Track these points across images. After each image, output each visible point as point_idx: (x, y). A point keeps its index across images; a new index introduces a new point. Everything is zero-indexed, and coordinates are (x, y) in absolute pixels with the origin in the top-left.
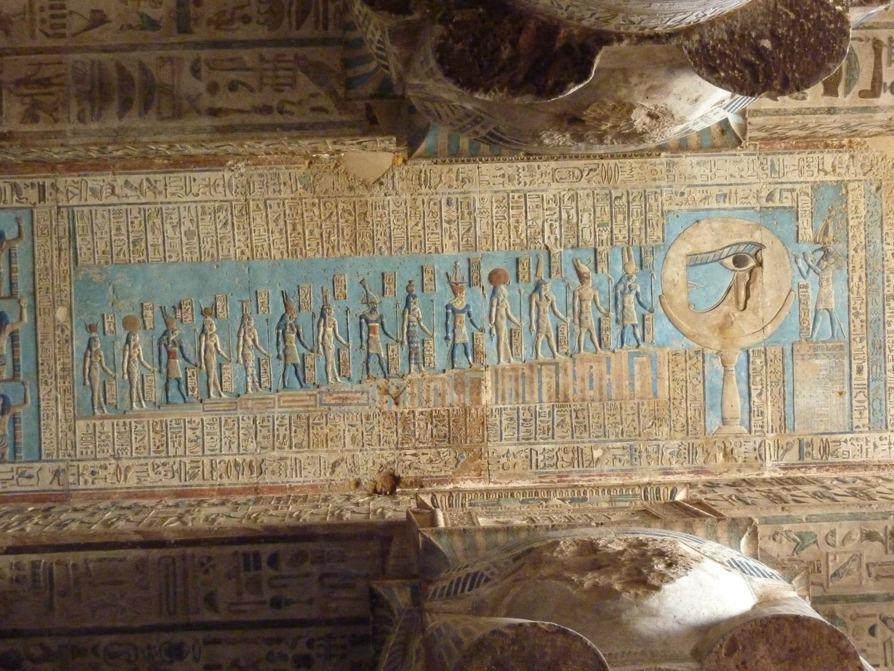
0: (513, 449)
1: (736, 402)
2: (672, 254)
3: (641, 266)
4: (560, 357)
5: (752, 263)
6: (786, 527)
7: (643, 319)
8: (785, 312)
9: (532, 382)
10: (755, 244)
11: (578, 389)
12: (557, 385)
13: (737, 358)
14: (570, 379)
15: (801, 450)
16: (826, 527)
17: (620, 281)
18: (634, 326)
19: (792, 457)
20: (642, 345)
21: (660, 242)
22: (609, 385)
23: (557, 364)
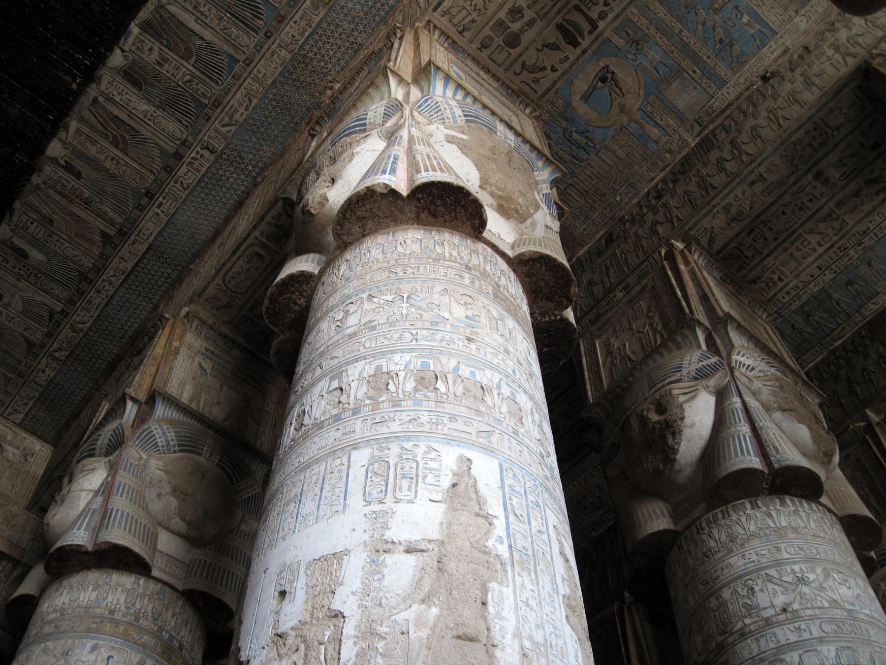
0: (584, 226)
1: (655, 132)
2: (574, 104)
3: (567, 120)
4: (569, 181)
5: (609, 76)
6: (715, 210)
7: (587, 137)
8: (642, 80)
9: (568, 199)
10: (604, 68)
11: (587, 184)
12: (579, 191)
13: (639, 115)
14: (582, 184)
15: (698, 123)
16: (732, 196)
17: (564, 133)
18: (586, 143)
19: (697, 128)
20: (597, 147)
21: (565, 104)
22: (598, 172)
23: (571, 184)
